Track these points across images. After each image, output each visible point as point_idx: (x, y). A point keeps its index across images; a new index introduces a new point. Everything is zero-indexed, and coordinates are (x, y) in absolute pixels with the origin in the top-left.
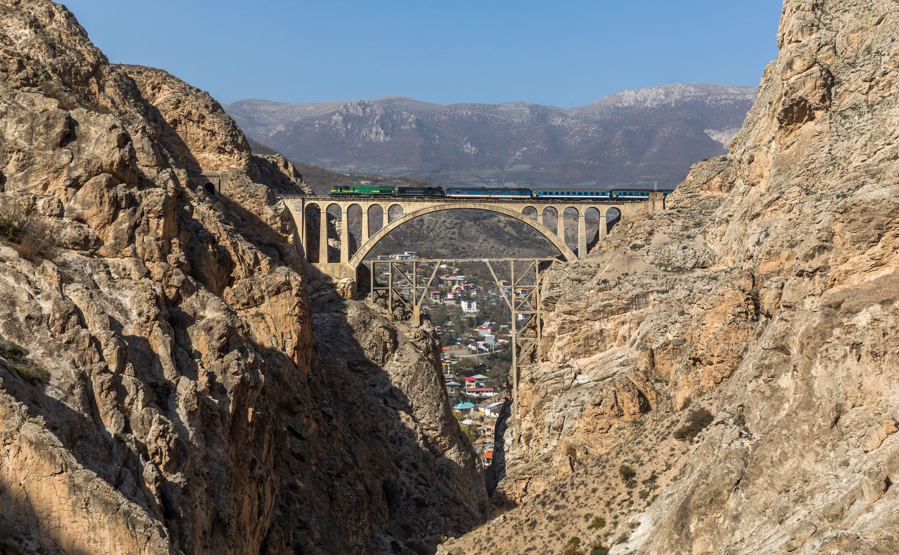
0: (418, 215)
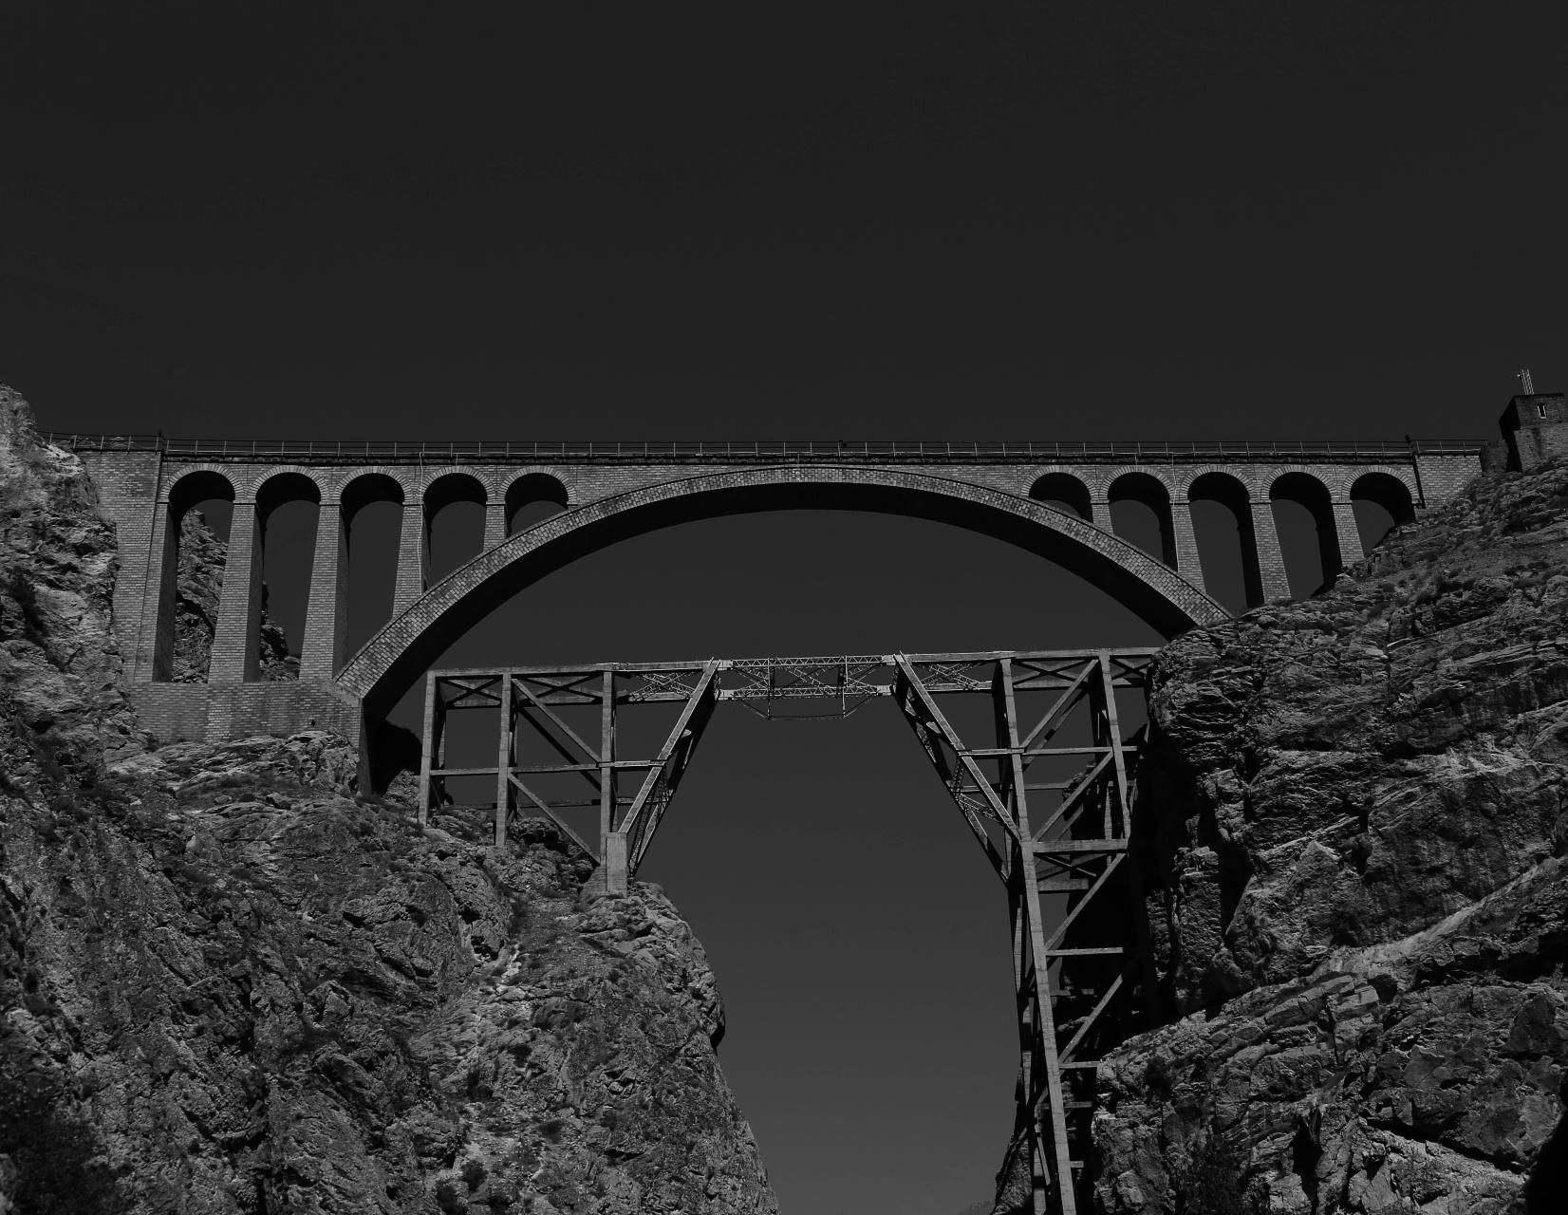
0: (623, 507)
